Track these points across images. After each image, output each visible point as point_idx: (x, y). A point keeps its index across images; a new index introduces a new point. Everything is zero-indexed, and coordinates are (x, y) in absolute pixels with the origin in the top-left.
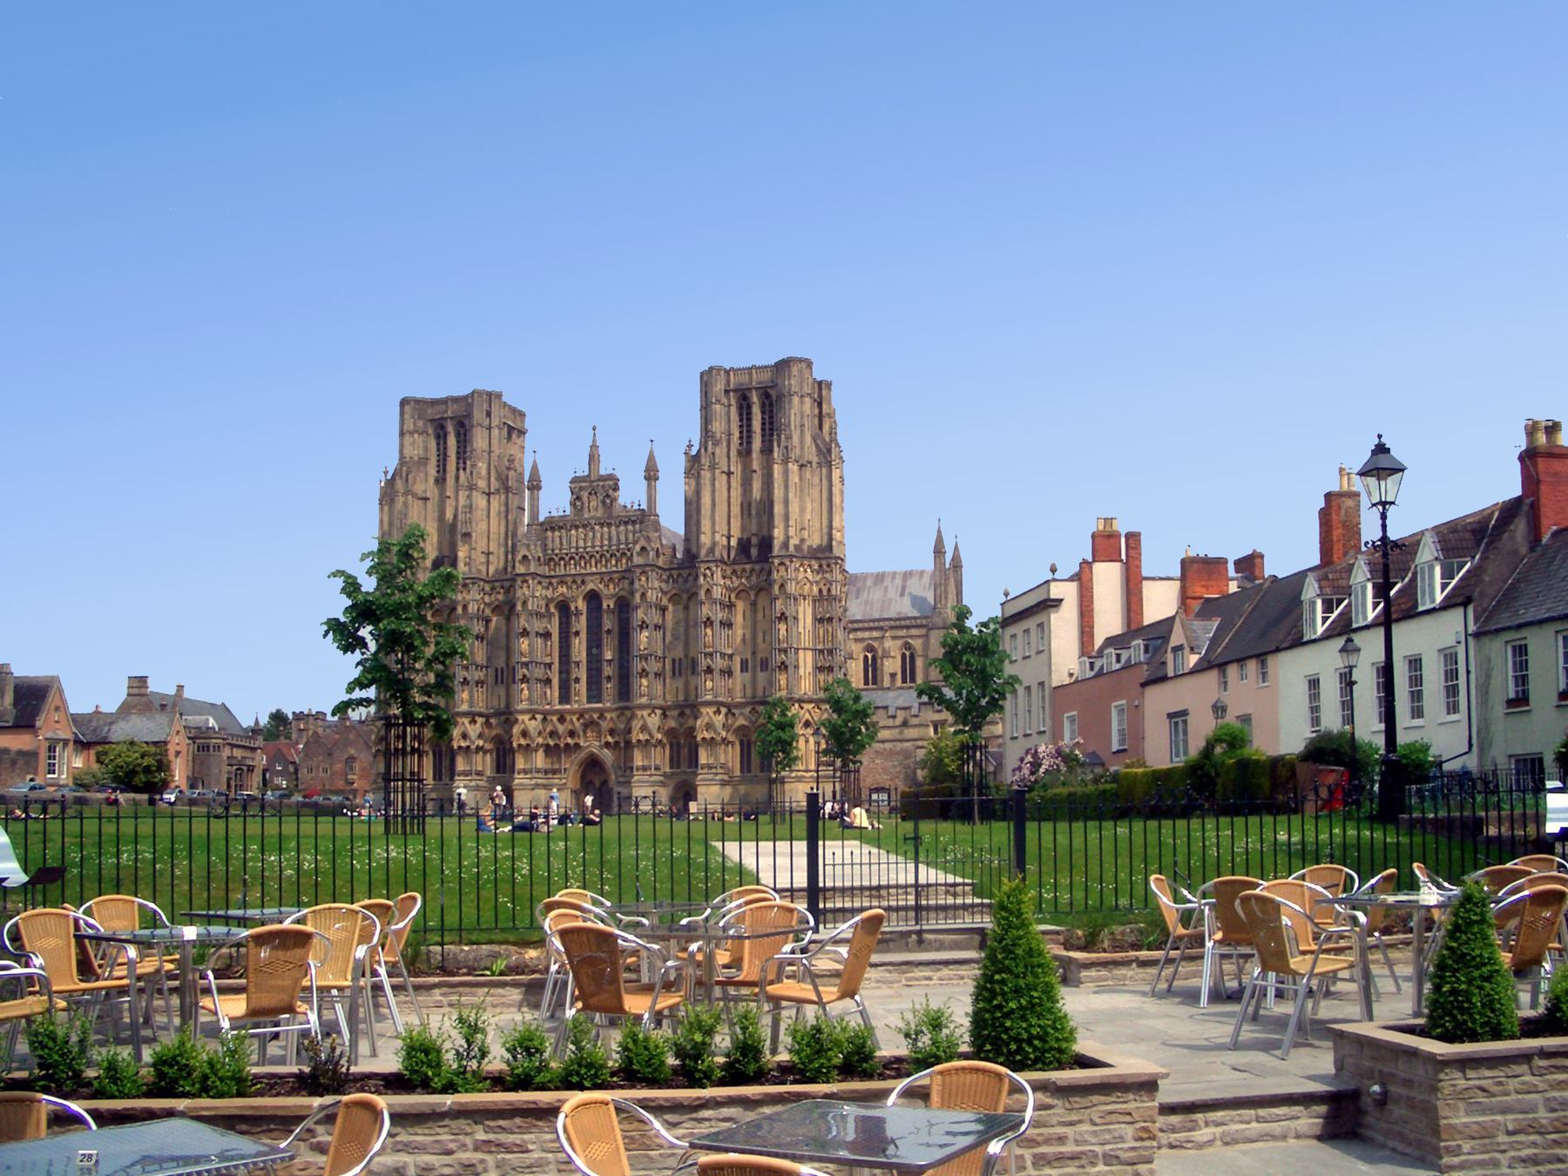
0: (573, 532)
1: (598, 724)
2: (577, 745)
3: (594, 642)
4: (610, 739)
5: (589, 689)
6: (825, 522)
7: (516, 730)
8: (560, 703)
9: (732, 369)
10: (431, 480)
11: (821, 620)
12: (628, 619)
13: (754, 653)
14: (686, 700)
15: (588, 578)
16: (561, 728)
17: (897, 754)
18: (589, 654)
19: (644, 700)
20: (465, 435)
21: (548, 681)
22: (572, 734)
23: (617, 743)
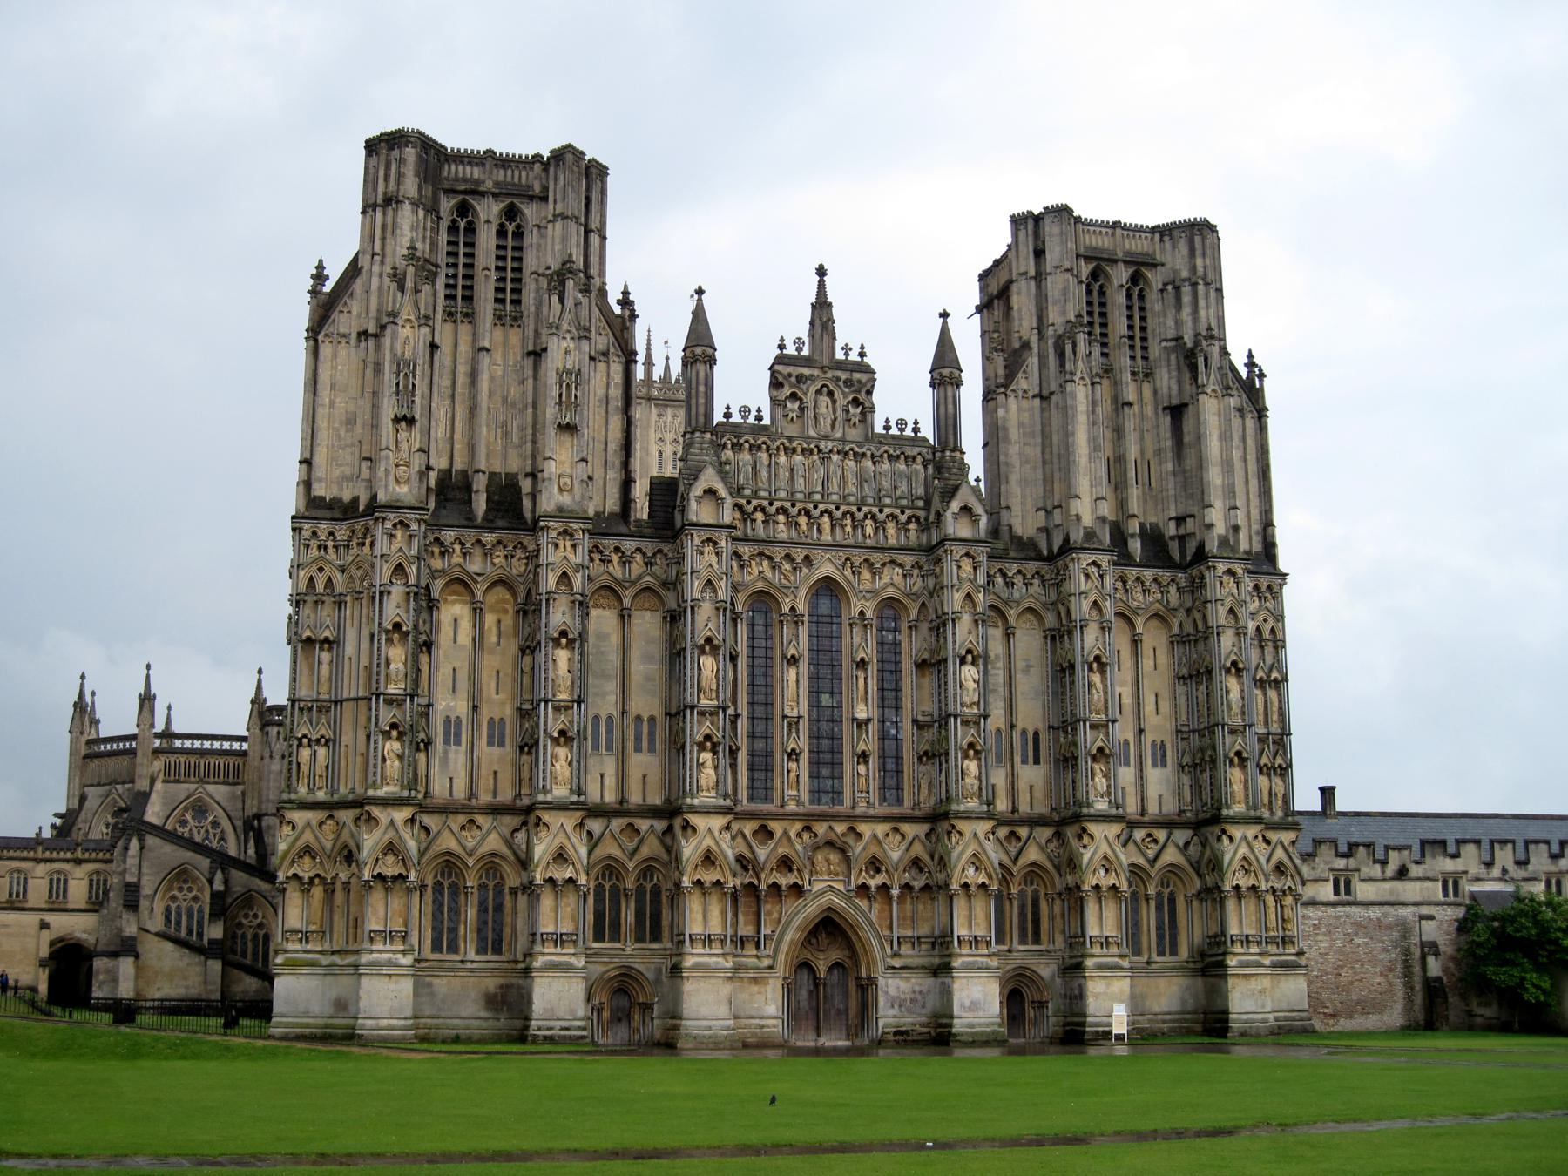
0: (782, 459)
1: (843, 851)
2: (797, 890)
3: (825, 679)
4: (864, 878)
7: (690, 850)
10: (440, 309)
12: (896, 644)
13: (1141, 731)
14: (1014, 810)
15: (817, 554)
16: (762, 853)
17: (1390, 927)
18: (815, 705)
19: (972, 804)
20: (519, 234)
21: (733, 753)
22: (786, 864)
23: (884, 888)
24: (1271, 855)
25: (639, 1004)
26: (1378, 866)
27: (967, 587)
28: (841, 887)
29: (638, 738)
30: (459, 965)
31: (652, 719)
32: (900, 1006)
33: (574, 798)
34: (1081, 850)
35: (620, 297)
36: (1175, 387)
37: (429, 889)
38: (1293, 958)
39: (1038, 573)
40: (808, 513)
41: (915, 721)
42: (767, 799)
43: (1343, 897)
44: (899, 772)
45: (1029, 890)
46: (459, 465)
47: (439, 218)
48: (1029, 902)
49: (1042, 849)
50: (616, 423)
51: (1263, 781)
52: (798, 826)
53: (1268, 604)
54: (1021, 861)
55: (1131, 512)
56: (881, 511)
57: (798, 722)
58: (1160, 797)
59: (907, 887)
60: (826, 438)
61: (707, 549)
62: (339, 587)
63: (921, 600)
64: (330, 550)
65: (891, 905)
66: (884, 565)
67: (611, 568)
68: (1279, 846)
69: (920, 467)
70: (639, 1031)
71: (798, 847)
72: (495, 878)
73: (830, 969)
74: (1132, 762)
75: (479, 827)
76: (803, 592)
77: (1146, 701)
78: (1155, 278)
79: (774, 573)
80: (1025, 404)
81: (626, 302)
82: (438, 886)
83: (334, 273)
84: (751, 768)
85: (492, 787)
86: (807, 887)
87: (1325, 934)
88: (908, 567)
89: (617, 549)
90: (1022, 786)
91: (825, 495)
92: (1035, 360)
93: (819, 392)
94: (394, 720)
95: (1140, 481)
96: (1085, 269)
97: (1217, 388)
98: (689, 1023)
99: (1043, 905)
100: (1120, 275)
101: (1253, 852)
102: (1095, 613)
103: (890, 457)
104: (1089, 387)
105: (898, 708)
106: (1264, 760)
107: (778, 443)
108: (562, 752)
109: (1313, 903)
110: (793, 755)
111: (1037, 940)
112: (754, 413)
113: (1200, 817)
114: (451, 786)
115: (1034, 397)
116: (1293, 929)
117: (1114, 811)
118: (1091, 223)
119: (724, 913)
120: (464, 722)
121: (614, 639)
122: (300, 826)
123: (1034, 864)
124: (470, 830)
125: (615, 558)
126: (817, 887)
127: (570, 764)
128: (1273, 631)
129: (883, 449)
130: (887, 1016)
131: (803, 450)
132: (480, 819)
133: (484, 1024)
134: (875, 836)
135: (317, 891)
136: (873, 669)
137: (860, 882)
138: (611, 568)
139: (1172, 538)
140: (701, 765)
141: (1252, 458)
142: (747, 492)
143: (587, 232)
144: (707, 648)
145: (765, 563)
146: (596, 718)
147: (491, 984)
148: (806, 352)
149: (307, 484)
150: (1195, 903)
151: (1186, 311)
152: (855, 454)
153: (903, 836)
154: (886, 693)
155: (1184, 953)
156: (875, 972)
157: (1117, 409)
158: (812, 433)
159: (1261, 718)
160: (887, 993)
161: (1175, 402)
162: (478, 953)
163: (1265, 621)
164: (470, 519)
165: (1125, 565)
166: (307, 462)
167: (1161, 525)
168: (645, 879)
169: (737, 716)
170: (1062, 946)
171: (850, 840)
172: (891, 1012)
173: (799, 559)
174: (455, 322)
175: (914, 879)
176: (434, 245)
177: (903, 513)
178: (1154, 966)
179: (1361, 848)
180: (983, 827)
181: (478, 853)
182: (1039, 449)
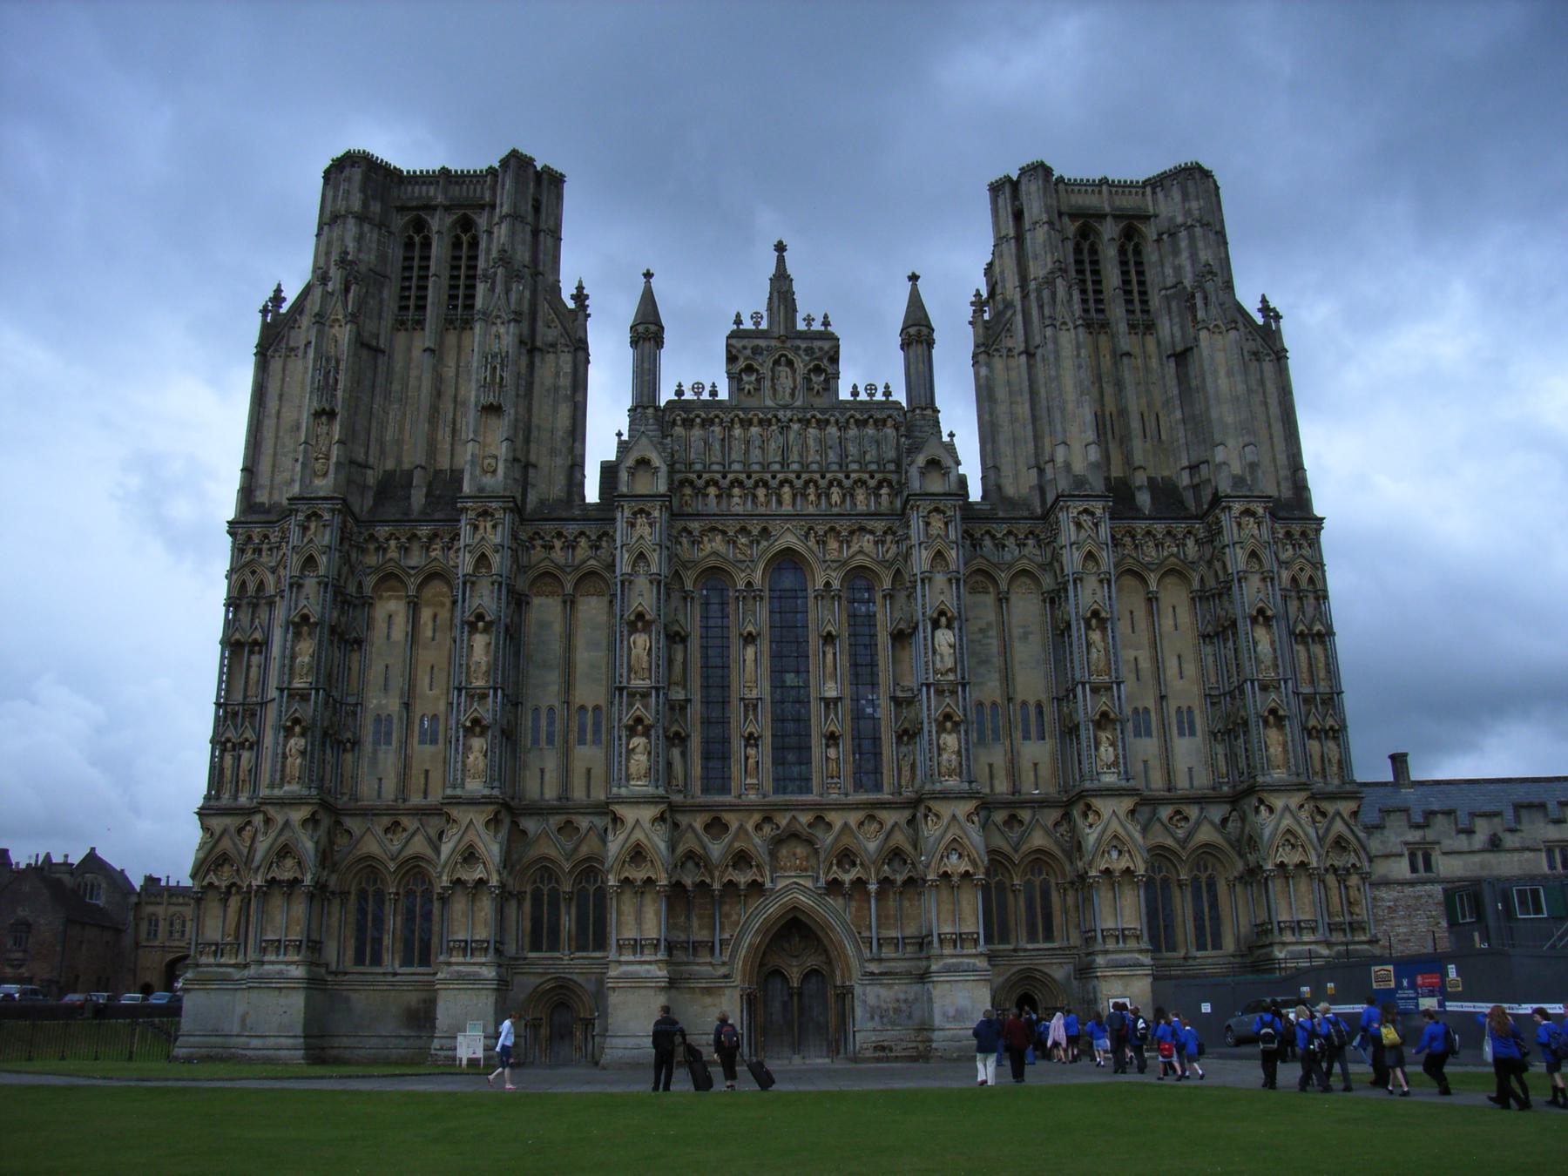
0: (737, 432)
1: (809, 842)
5: (778, 761)
6: (1282, 459)
8: (706, 790)
9: (1061, 179)
10: (388, 321)
11: (1302, 638)
12: (871, 616)
13: (1163, 698)
16: (716, 849)
18: (778, 684)
19: (952, 783)
20: (474, 244)
21: (679, 739)
23: (860, 883)
24: (1328, 830)
25: (581, 1019)
26: (1463, 837)
27: (938, 544)
28: (809, 884)
29: (582, 730)
30: (381, 978)
31: (597, 708)
32: (881, 1017)
33: (486, 792)
34: (1087, 830)
35: (575, 292)
36: (1178, 334)
37: (353, 897)
38: (1366, 947)
39: (1031, 532)
40: (766, 484)
41: (894, 699)
42: (725, 790)
43: (1422, 874)
44: (877, 755)
45: (1037, 881)
46: (406, 466)
47: (390, 233)
48: (1038, 894)
49: (1047, 832)
50: (564, 411)
51: (1314, 746)
52: (757, 817)
53: (1304, 552)
54: (1025, 848)
55: (1137, 464)
56: (848, 477)
57: (755, 706)
58: (1190, 769)
59: (885, 882)
60: (785, 407)
61: (639, 521)
62: (271, 589)
63: (895, 568)
64: (264, 554)
65: (869, 902)
66: (852, 533)
67: (553, 555)
68: (1338, 818)
69: (890, 431)
70: (580, 1049)
71: (757, 841)
72: (423, 883)
73: (806, 977)
74: (1154, 733)
75: (404, 830)
76: (761, 566)
77: (1168, 664)
78: (1150, 231)
79: (728, 549)
80: (1013, 363)
81: (580, 297)
82: (362, 895)
83: (291, 295)
84: (706, 757)
85: (422, 786)
86: (768, 885)
87: (1403, 918)
88: (880, 533)
89: (560, 535)
90: (1026, 764)
91: (784, 464)
92: (1019, 317)
93: (777, 362)
94: (297, 715)
95: (1148, 434)
96: (1071, 228)
97: (1219, 322)
98: (615, 1041)
99: (1055, 898)
100: (1109, 231)
101: (1299, 824)
102: (1091, 565)
103: (857, 422)
104: (1072, 331)
105: (874, 685)
106: (1312, 722)
107: (732, 415)
108: (478, 743)
109: (1386, 883)
110: (752, 741)
111: (1049, 937)
112: (708, 389)
113: (1239, 788)
114: (380, 787)
115: (1020, 354)
116: (1362, 913)
117: (1123, 783)
118: (1075, 183)
119: (658, 914)
120: (395, 721)
121: (558, 627)
122: (217, 834)
123: (1039, 851)
124: (394, 832)
125: (558, 544)
126: (781, 884)
127: (485, 756)
128: (1311, 580)
129: (848, 414)
130: (865, 1032)
131: (761, 422)
132: (405, 821)
133: (404, 1043)
134: (846, 825)
135: (234, 902)
136: (843, 645)
137: (831, 877)
138: (553, 555)
139: (1184, 488)
140: (630, 752)
141: (1273, 401)
142: (698, 467)
143: (536, 233)
144: (640, 625)
145: (719, 537)
146: (537, 710)
147: (413, 998)
148: (764, 325)
149: (247, 492)
150: (1239, 888)
151: (1185, 254)
152: (818, 421)
153: (881, 824)
154: (859, 669)
155: (1229, 945)
156: (850, 979)
157: (1115, 364)
158: (769, 403)
159: (1305, 676)
160: (864, 1002)
161: (1179, 349)
162: (403, 964)
163: (1302, 570)
164: (406, 514)
165: (1134, 519)
166: (249, 470)
167: (1174, 478)
168: (588, 881)
169: (688, 701)
170: (1078, 943)
171: (819, 833)
172: (870, 1025)
173: (755, 532)
174: (406, 330)
175: (895, 871)
176: (382, 257)
177: (872, 477)
178: (1191, 962)
179: (1439, 816)
180: (963, 808)
181: (401, 857)
182: (1027, 406)
